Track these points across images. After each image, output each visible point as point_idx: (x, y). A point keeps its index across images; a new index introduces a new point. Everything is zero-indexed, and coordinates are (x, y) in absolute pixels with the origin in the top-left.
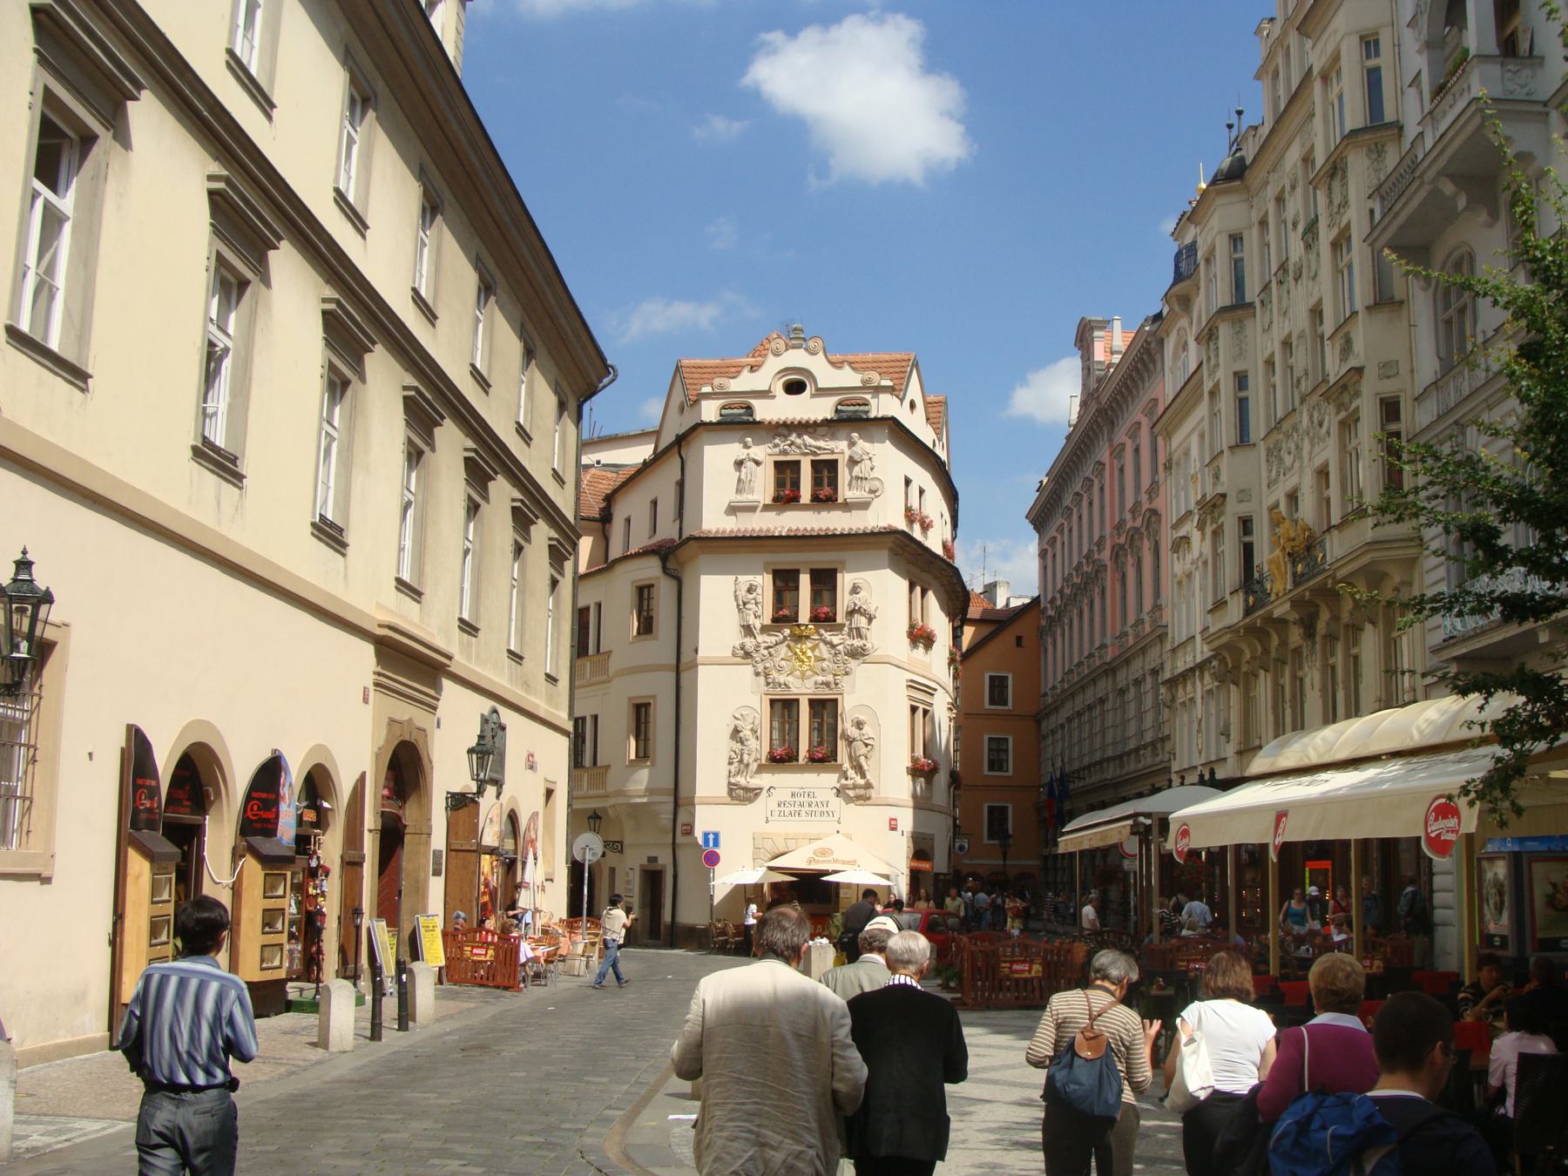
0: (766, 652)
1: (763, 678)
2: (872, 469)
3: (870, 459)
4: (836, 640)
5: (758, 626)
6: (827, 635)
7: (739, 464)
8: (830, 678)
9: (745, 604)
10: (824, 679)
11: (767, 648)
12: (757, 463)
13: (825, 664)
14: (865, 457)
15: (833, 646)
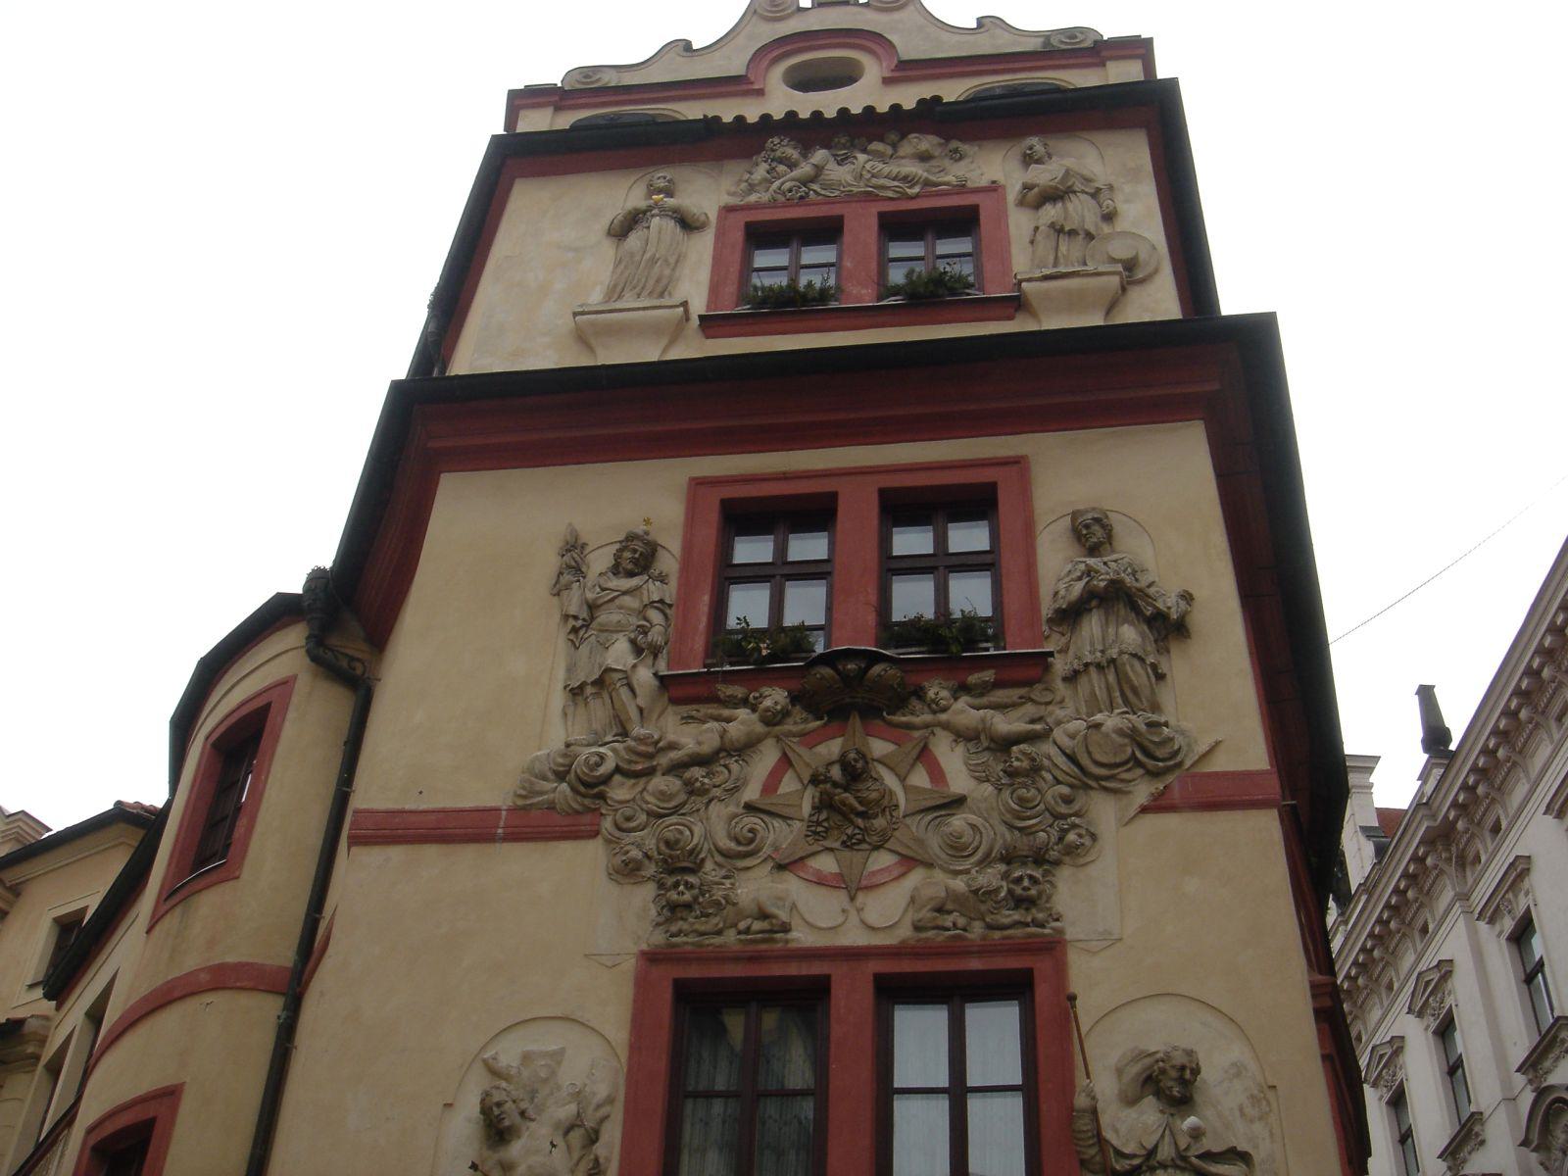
0: (669, 784)
1: (649, 890)
2: (1109, 217)
3: (1095, 194)
4: (1005, 724)
5: (644, 676)
6: (964, 712)
7: (628, 225)
8: (990, 877)
9: (593, 607)
10: (959, 884)
11: (677, 768)
12: (687, 224)
13: (958, 822)
14: (1078, 186)
15: (1003, 745)
